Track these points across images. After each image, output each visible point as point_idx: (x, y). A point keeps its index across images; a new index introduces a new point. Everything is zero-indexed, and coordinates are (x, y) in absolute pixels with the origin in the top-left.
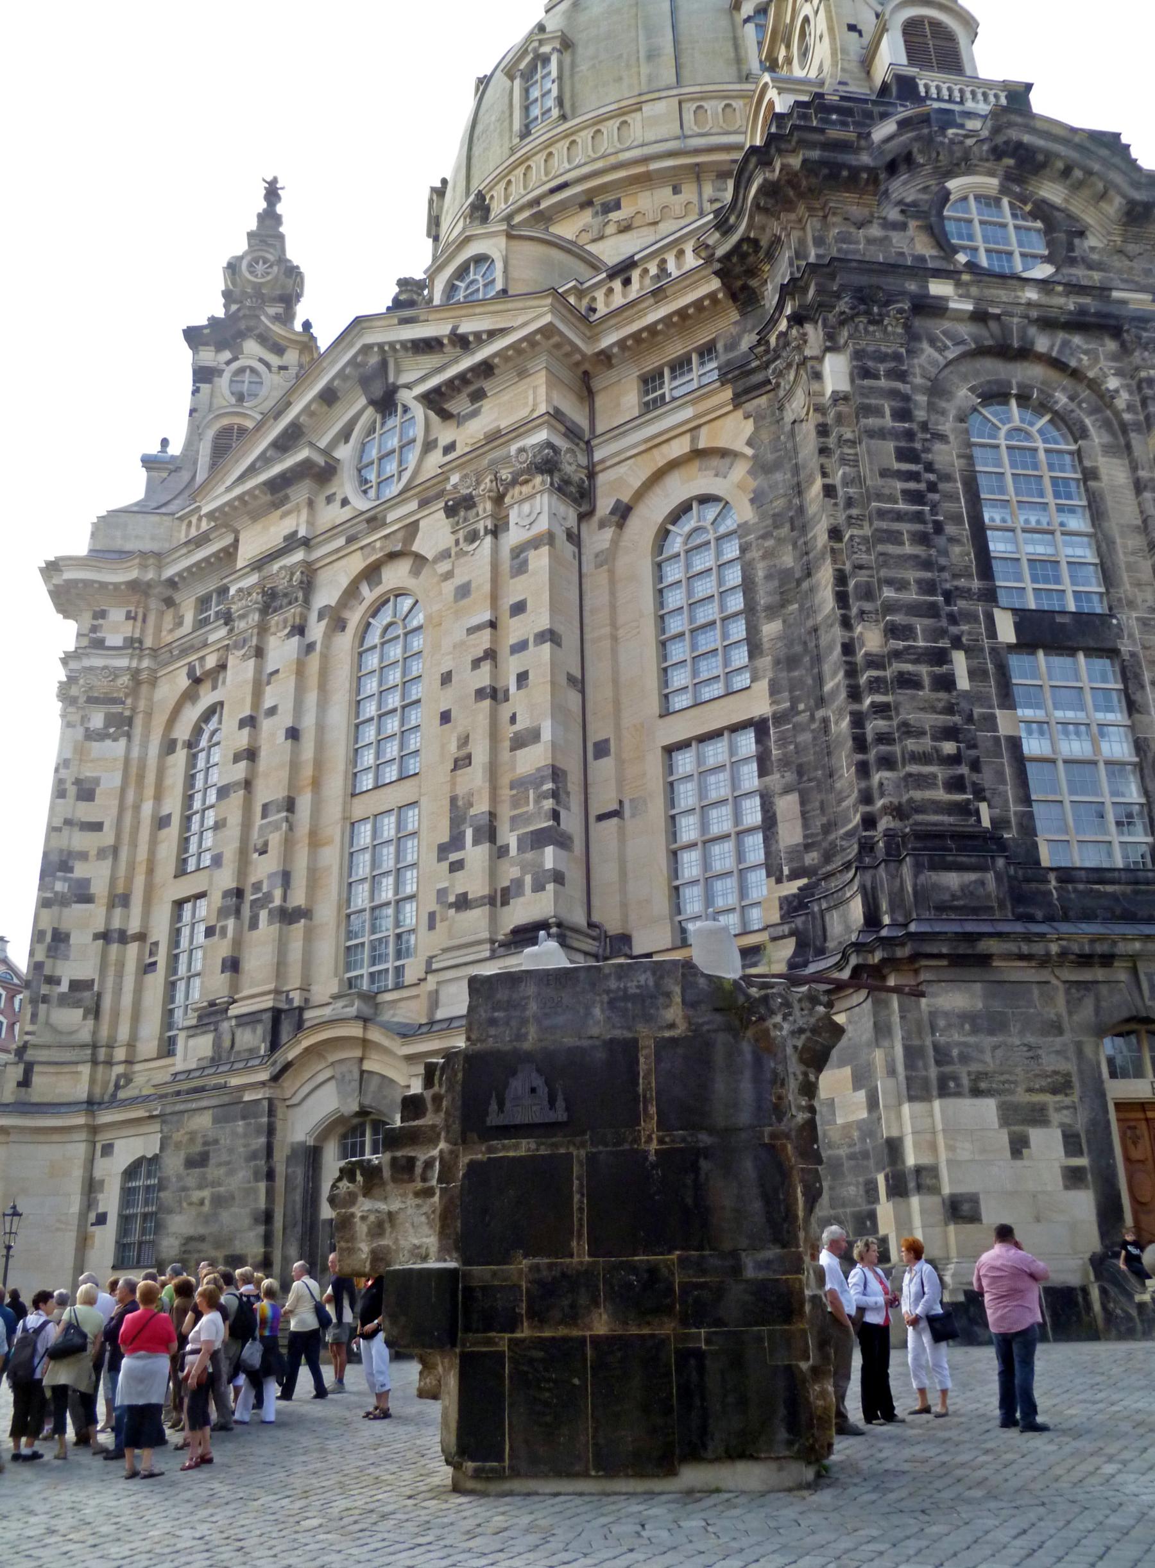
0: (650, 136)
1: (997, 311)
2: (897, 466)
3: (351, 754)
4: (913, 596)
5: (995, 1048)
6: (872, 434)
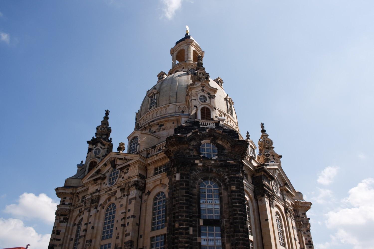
0: (170, 112)
1: (207, 165)
2: (185, 194)
3: (102, 232)
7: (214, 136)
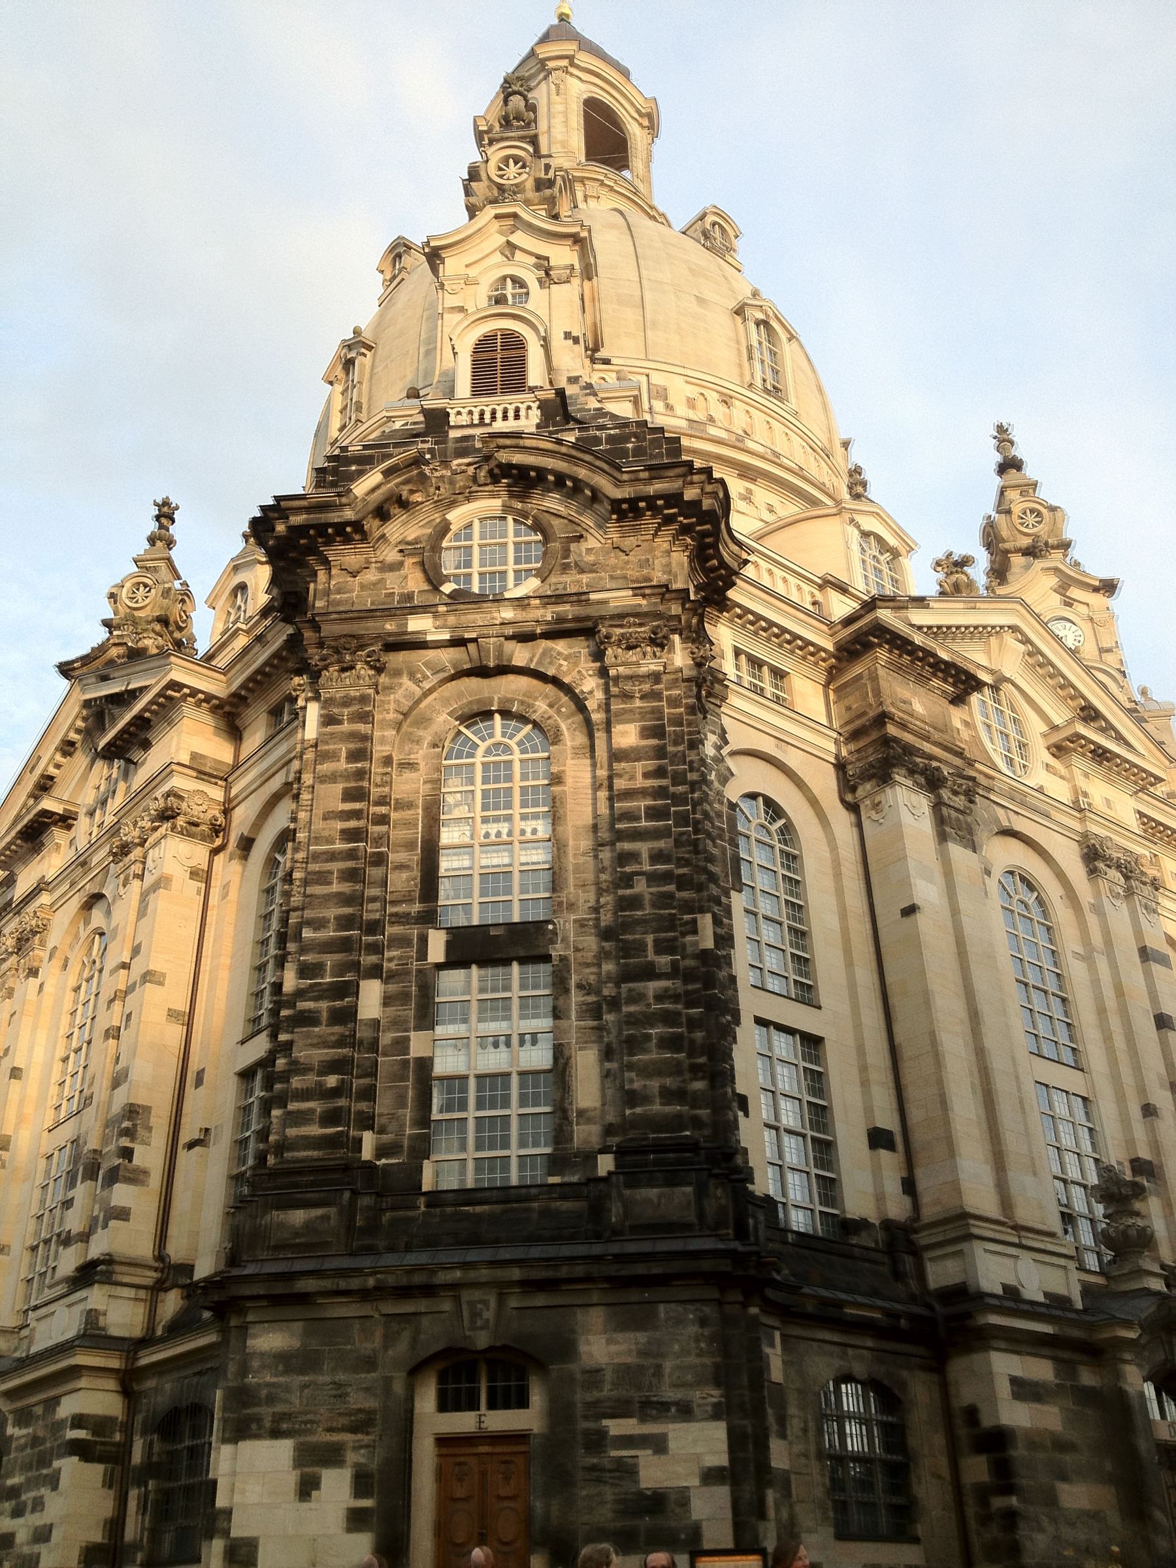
1: (474, 635)
4: (330, 933)
5: (304, 1386)
6: (323, 779)
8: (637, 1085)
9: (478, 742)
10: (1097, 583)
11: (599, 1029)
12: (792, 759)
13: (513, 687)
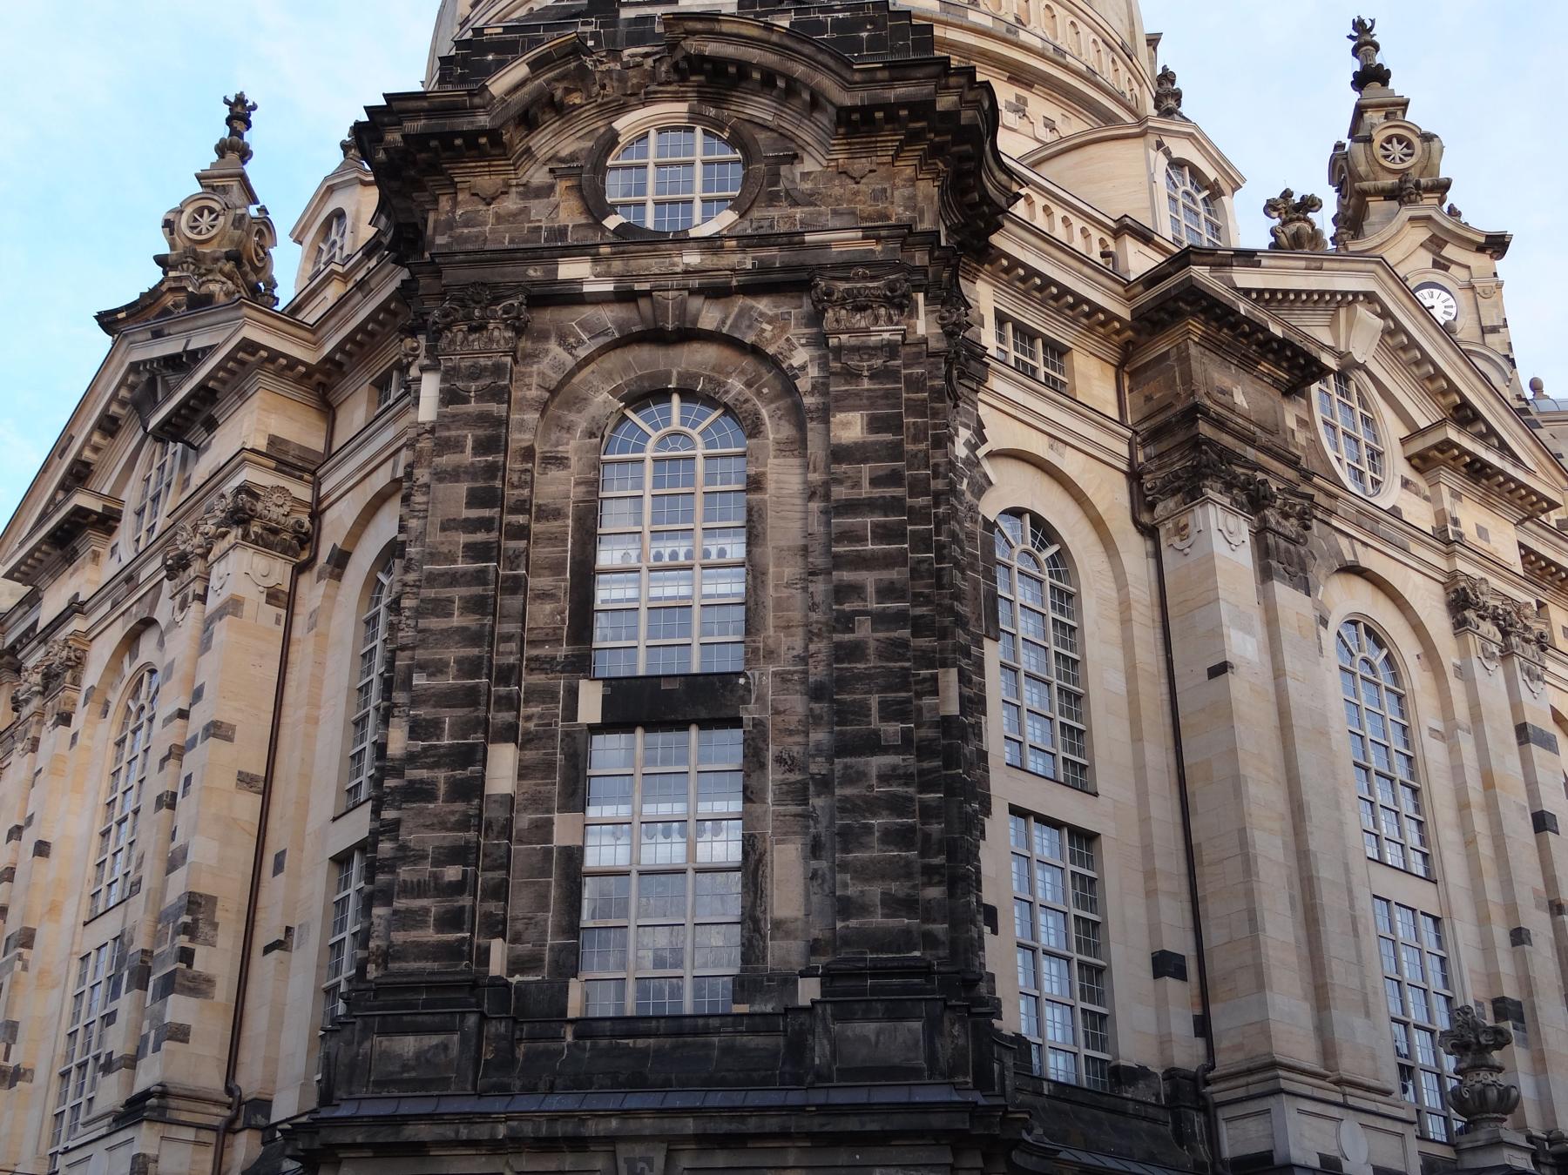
1: (646, 286)
4: (449, 681)
6: (441, 476)
7: (698, 63)
8: (851, 891)
9: (649, 430)
10: (1482, 240)
11: (805, 816)
12: (1070, 463)
13: (698, 357)
